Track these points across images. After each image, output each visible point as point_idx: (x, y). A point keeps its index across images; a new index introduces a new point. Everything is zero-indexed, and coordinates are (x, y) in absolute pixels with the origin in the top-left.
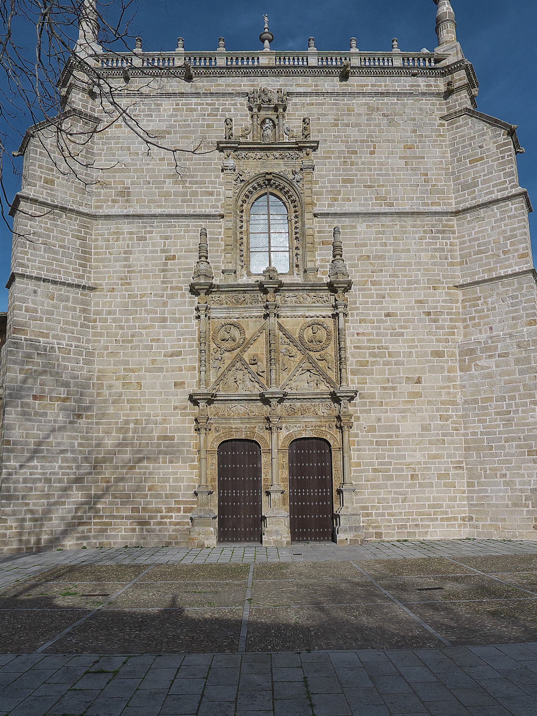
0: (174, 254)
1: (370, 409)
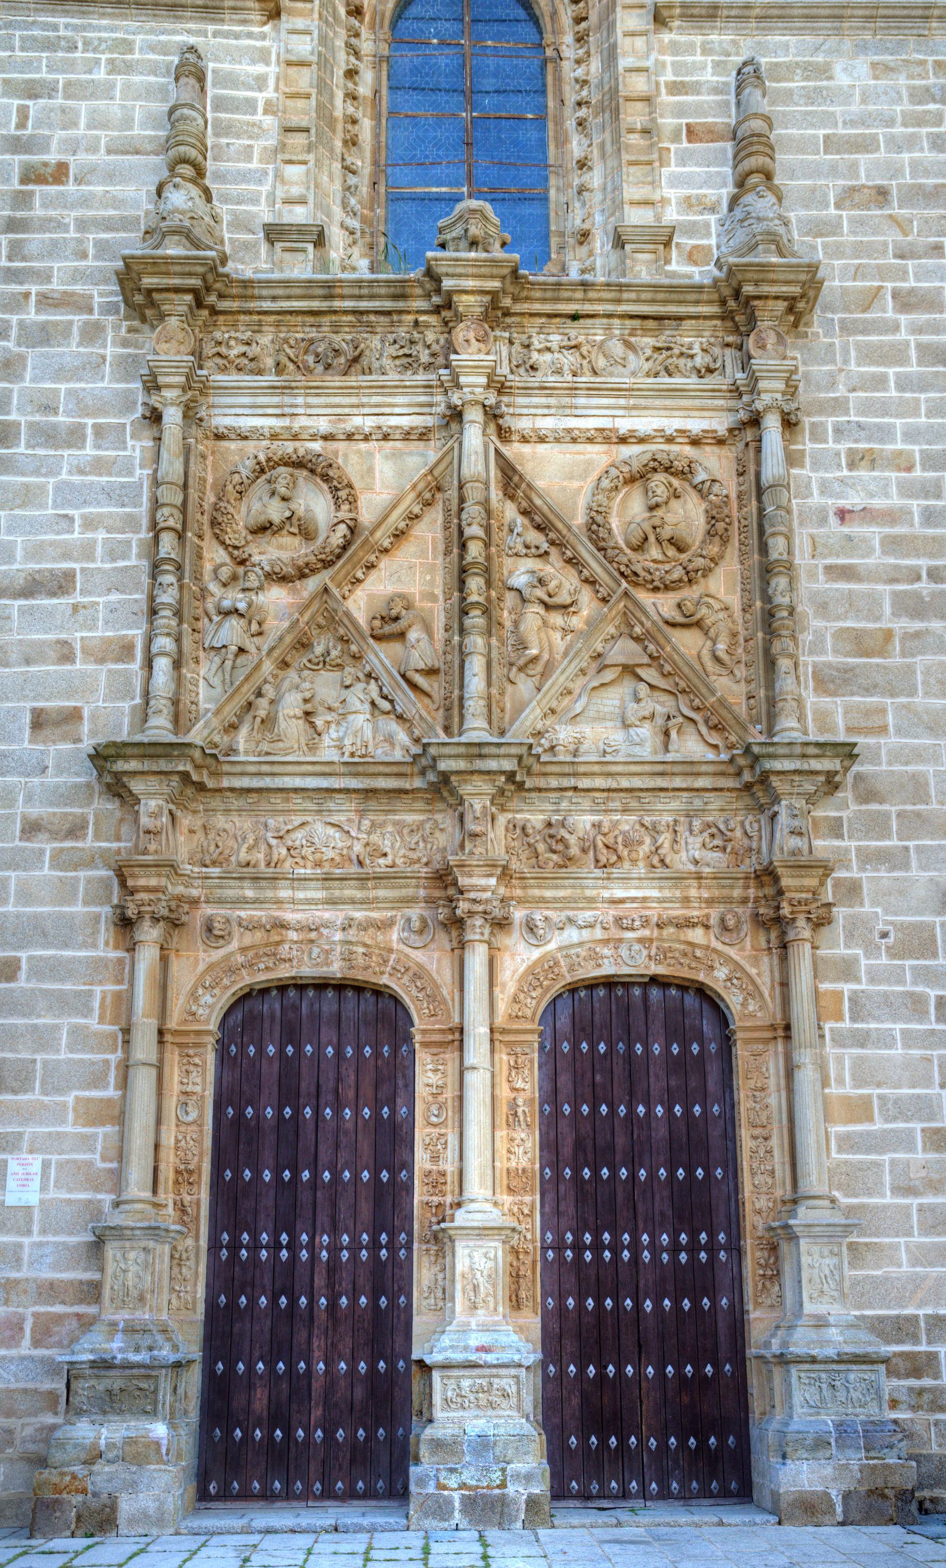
0: (63, 158)
1: (907, 849)
